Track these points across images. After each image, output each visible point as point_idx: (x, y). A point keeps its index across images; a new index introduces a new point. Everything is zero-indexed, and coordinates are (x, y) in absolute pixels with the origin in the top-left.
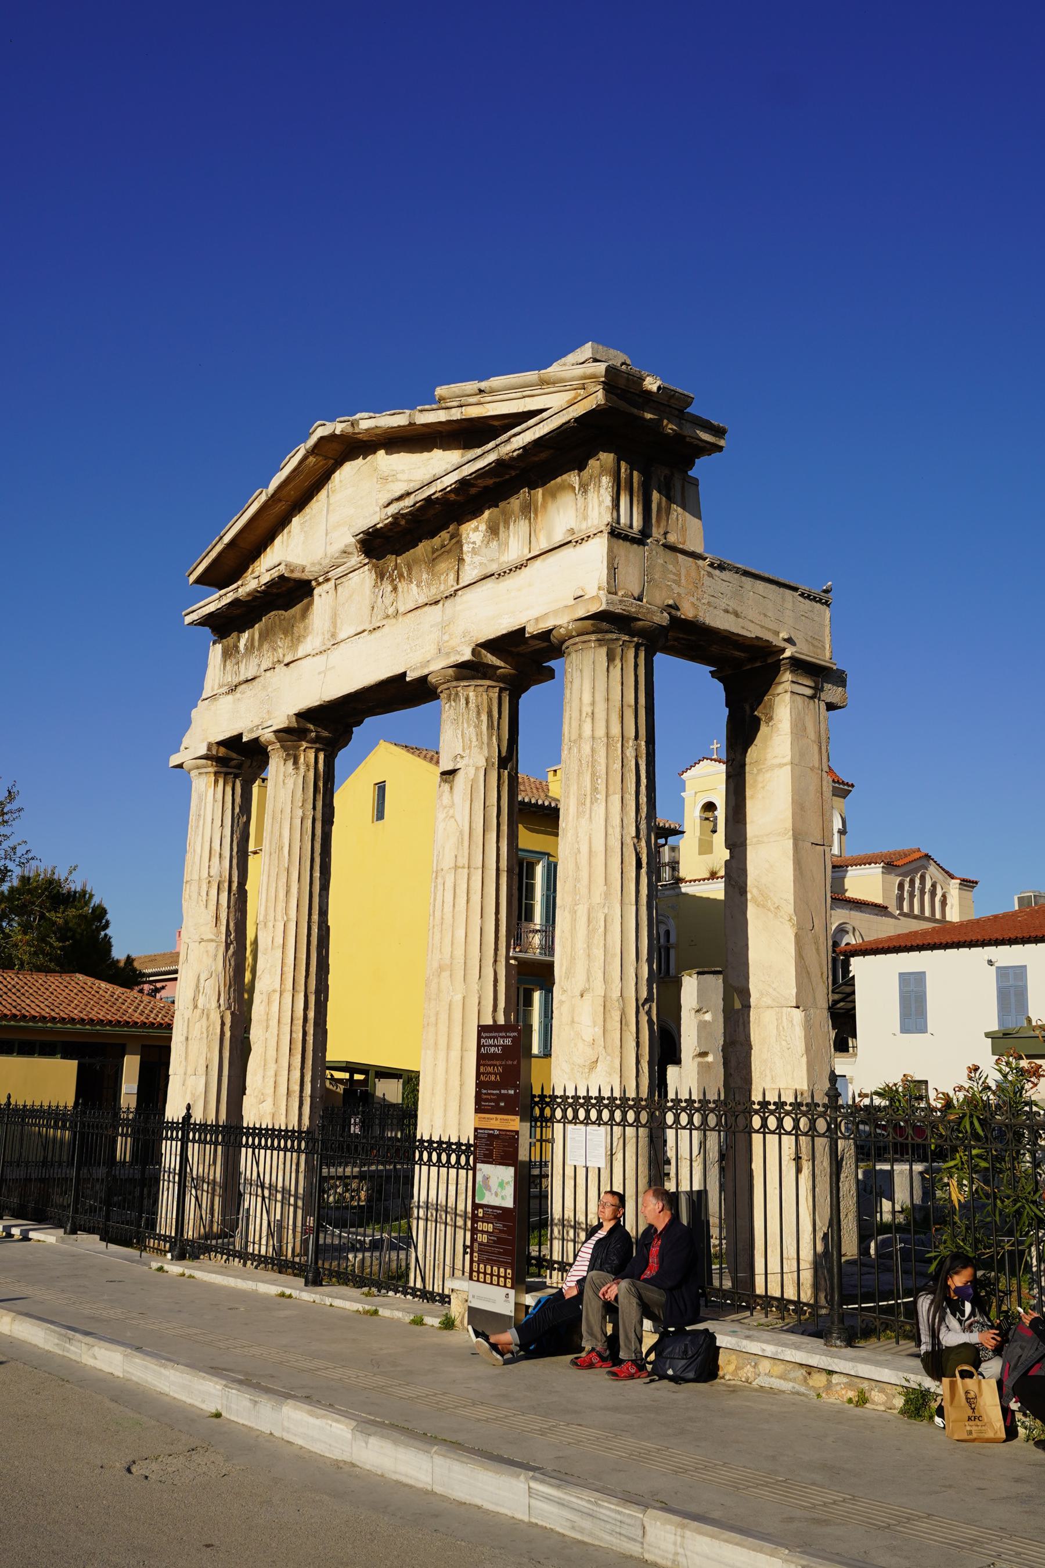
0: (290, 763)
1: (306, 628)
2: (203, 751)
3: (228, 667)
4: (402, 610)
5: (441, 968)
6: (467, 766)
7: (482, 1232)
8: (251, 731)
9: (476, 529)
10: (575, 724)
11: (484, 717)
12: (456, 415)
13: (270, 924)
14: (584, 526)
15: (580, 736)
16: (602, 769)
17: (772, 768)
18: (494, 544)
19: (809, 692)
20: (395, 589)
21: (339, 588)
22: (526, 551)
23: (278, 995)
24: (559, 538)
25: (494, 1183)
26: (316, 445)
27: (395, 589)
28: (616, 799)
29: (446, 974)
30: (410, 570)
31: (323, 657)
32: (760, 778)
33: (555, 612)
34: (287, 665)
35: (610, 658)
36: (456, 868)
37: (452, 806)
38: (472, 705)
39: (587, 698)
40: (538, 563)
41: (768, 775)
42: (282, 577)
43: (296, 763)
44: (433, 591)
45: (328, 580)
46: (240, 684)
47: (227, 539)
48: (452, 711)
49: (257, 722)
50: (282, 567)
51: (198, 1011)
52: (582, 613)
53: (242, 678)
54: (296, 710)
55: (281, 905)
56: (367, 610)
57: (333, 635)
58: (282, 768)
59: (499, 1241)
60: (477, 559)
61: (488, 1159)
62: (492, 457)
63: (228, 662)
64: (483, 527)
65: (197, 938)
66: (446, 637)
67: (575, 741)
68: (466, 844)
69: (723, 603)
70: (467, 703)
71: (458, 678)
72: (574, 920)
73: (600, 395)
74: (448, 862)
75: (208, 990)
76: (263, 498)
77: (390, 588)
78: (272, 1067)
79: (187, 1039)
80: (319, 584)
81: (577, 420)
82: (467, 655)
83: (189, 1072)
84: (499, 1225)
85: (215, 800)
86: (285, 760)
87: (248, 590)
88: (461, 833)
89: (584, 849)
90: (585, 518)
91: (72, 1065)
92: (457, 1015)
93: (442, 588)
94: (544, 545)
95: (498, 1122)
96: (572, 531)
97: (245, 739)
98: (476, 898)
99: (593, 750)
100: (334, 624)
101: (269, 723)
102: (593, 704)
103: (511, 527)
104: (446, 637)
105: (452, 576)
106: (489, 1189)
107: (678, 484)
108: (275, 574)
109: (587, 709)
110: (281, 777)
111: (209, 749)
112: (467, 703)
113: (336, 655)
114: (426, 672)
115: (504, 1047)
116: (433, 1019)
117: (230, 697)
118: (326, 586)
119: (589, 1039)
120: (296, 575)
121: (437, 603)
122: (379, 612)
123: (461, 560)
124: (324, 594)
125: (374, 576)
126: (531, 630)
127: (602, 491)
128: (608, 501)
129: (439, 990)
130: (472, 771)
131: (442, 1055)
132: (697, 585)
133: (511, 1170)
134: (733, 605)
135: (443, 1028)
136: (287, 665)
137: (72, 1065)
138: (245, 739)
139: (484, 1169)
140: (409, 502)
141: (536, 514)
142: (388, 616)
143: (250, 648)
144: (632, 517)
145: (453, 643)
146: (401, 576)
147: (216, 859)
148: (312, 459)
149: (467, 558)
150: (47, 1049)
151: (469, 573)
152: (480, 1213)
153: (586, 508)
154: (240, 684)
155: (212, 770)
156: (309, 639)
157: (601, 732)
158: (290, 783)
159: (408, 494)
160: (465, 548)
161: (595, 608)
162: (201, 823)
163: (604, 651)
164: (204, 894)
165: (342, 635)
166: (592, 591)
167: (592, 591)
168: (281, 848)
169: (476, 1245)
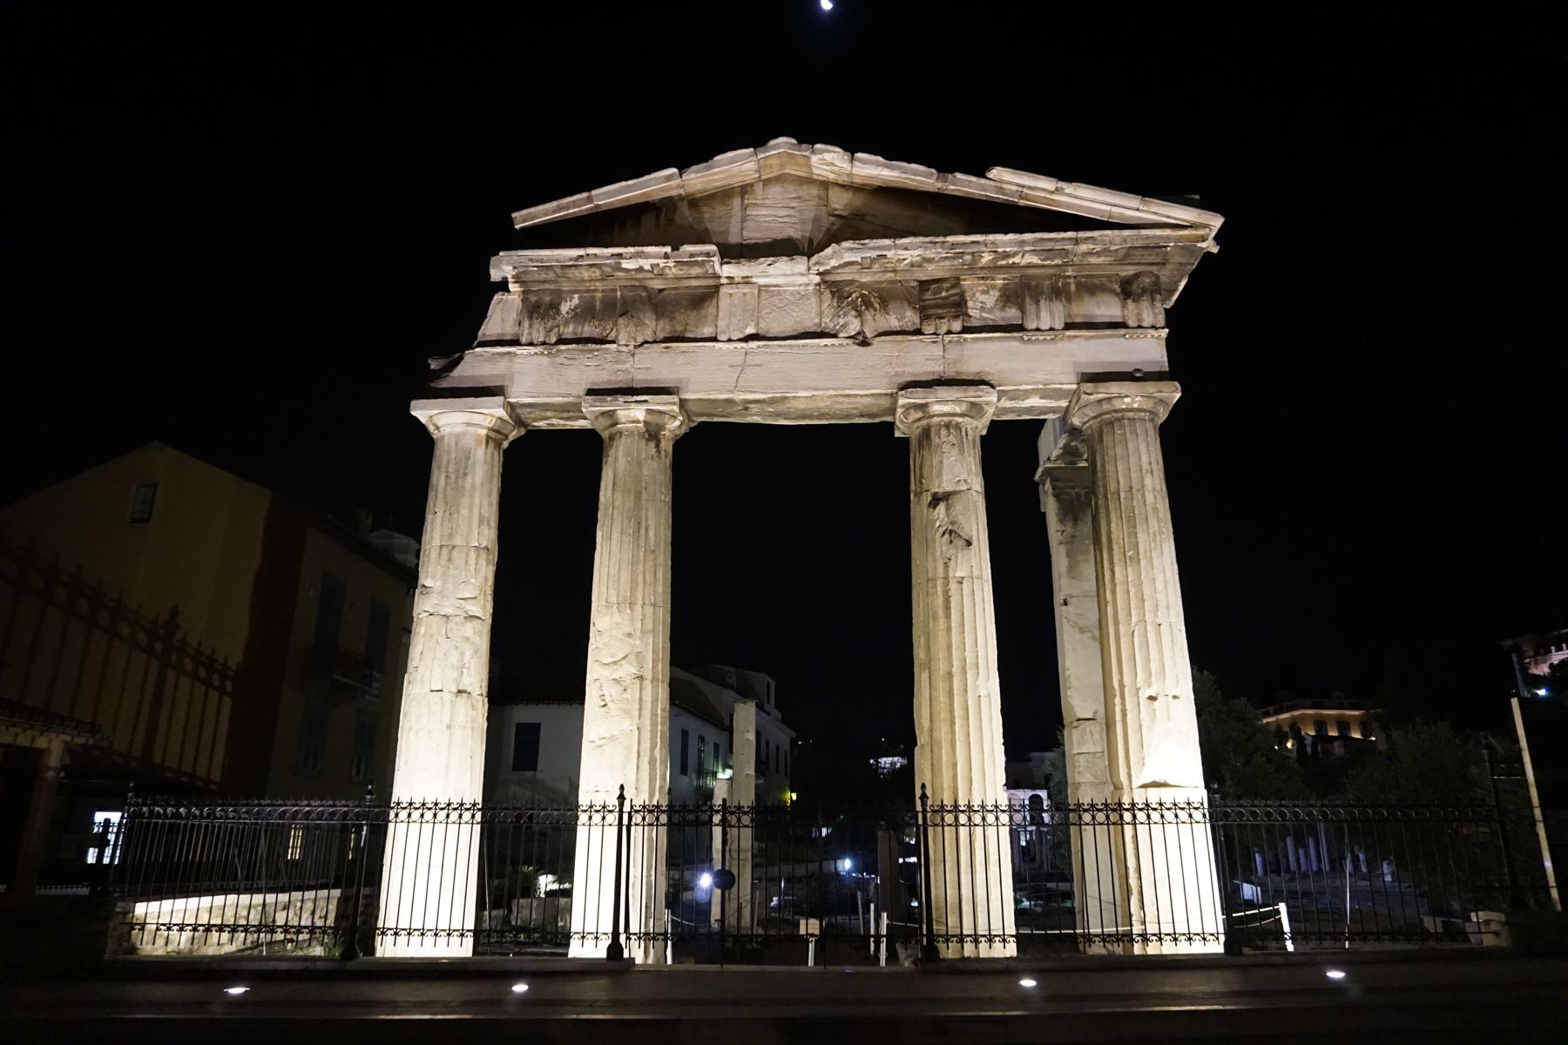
9: (986, 292)
13: (638, 608)
20: (860, 315)
43: (657, 446)
64: (995, 294)
71: (962, 415)
79: (449, 727)
90: (1139, 316)
117: (545, 360)
160: (970, 304)
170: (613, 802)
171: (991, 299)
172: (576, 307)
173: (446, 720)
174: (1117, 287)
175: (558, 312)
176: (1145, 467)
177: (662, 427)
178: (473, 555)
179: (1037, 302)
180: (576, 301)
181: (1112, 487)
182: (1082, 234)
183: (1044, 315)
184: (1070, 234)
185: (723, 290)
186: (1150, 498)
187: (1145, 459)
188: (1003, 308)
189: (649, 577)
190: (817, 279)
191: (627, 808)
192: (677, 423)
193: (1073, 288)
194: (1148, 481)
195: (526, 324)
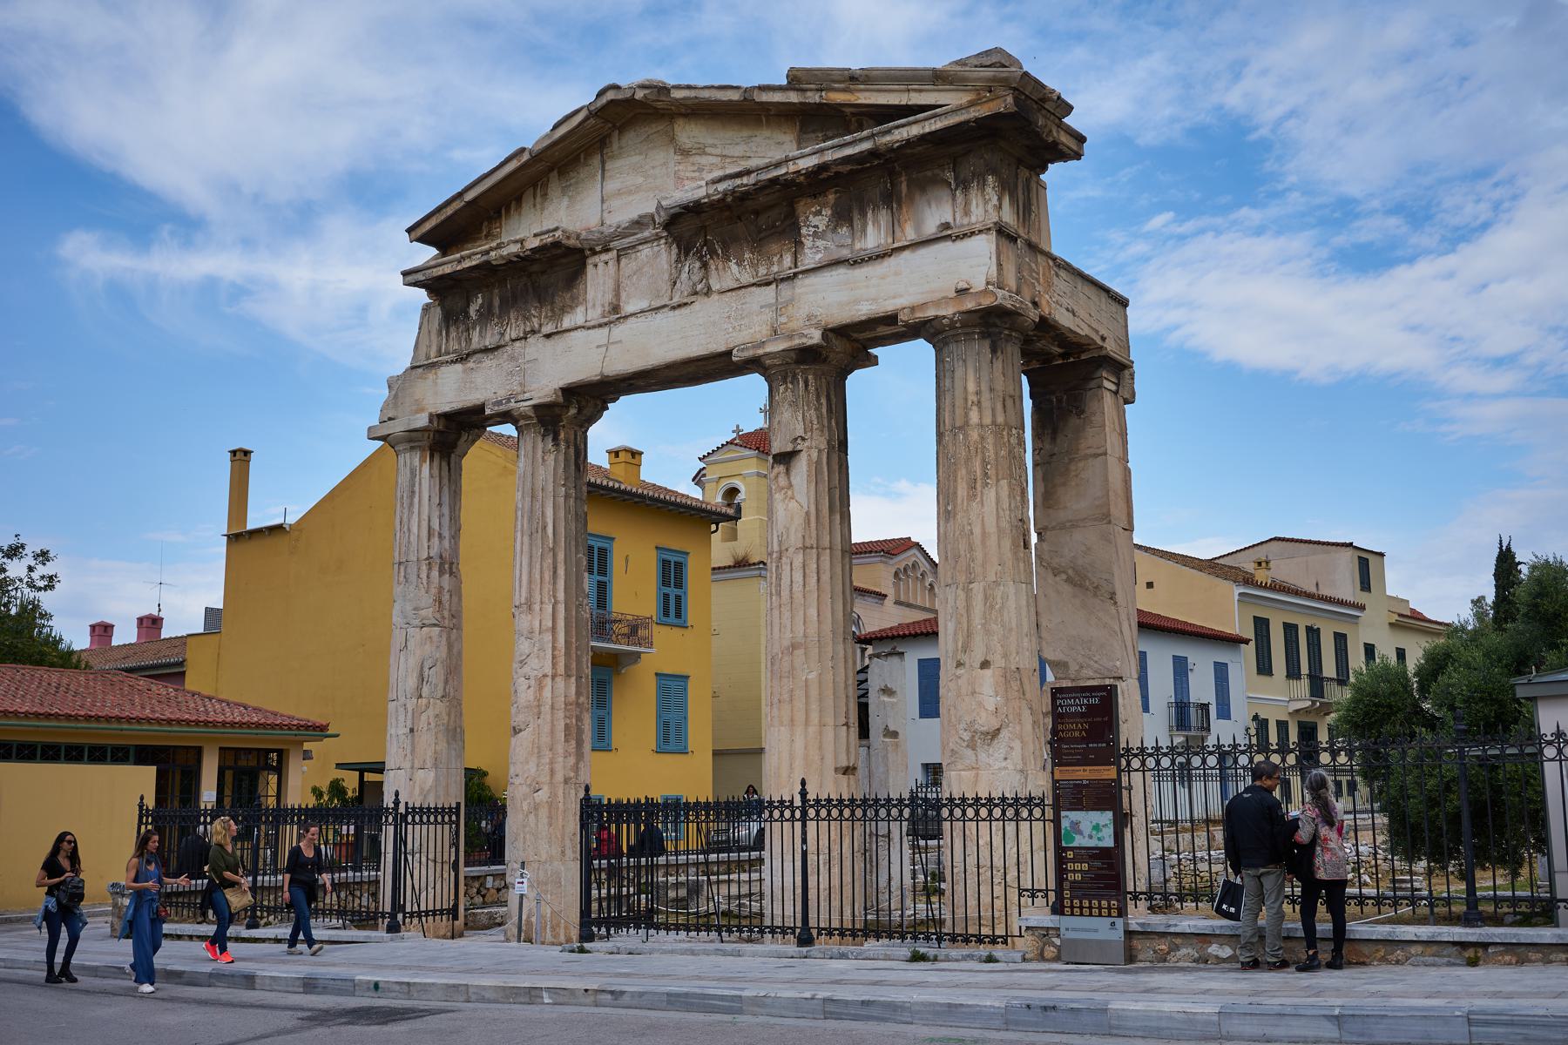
0: (549, 439)
1: (573, 299)
2: (422, 421)
3: (453, 334)
4: (715, 286)
5: (794, 646)
6: (810, 448)
7: (1074, 871)
8: (499, 403)
9: (818, 213)
10: (959, 412)
11: (823, 401)
12: (813, 98)
13: (537, 607)
14: (965, 221)
15: (967, 423)
16: (991, 454)
17: (1086, 457)
18: (844, 230)
19: (1113, 388)
20: (705, 266)
21: (624, 261)
22: (890, 240)
23: (549, 680)
24: (931, 227)
25: (1086, 827)
26: (603, 108)
27: (705, 266)
28: (1004, 483)
29: (799, 652)
30: (725, 248)
31: (605, 330)
32: (1073, 467)
33: (937, 303)
34: (548, 336)
35: (994, 351)
36: (805, 548)
37: (790, 486)
38: (812, 389)
39: (971, 387)
40: (906, 253)
41: (1081, 465)
42: (556, 244)
43: (555, 439)
44: (762, 271)
45: (607, 250)
46: (475, 352)
48: (789, 393)
49: (502, 394)
50: (557, 234)
51: (423, 701)
52: (970, 305)
53: (475, 344)
54: (562, 383)
55: (548, 587)
56: (665, 287)
57: (616, 308)
58: (540, 445)
59: (1098, 877)
60: (820, 243)
61: (1077, 805)
62: (866, 146)
63: (452, 329)
64: (827, 212)
65: (417, 622)
66: (783, 319)
67: (960, 428)
68: (813, 525)
69: (1065, 301)
70: (806, 386)
71: (799, 362)
72: (968, 599)
73: (1010, 99)
74: (795, 540)
75: (433, 680)
77: (698, 264)
78: (547, 755)
79: (412, 730)
80: (594, 253)
81: (977, 120)
82: (815, 337)
83: (417, 765)
84: (1098, 864)
85: (431, 476)
86: (544, 436)
88: (807, 513)
89: (977, 531)
90: (967, 213)
91: (151, 771)
92: (814, 693)
93: (775, 269)
94: (910, 234)
95: (1084, 774)
96: (946, 226)
98: (826, 577)
99: (982, 438)
100: (617, 295)
101: (527, 396)
102: (978, 393)
103: (870, 215)
104: (783, 319)
105: (788, 260)
106: (1080, 833)
107: (1034, 185)
109: (972, 398)
110: (540, 453)
111: (431, 421)
112: (806, 386)
113: (620, 331)
114: (760, 352)
115: (1088, 706)
116: (786, 696)
117: (459, 367)
118: (604, 257)
119: (991, 708)
120: (572, 242)
121: (768, 284)
122: (684, 285)
123: (799, 244)
124: (601, 265)
125: (675, 250)
127: (989, 190)
128: (995, 200)
129: (793, 668)
130: (815, 455)
131: (799, 730)
132: (1049, 285)
133: (1110, 814)
134: (1072, 305)
135: (799, 704)
136: (548, 336)
137: (151, 771)
138: (488, 412)
139: (1069, 817)
140: (752, 179)
141: (900, 205)
142: (696, 293)
143: (486, 315)
144: (1008, 216)
145: (793, 325)
146: (713, 253)
147: (436, 540)
148: (592, 121)
149: (808, 242)
150: (119, 755)
151: (810, 258)
152: (1070, 855)
153: (967, 204)
154: (475, 352)
155: (426, 443)
156: (580, 310)
157: (987, 420)
158: (551, 459)
159: (748, 172)
160: (804, 231)
161: (987, 302)
162: (416, 500)
163: (987, 343)
164: (424, 576)
165: (628, 308)
166: (979, 284)
167: (979, 284)
168: (545, 528)
169: (1066, 885)
170: (391, 805)
171: (821, 222)
172: (482, 306)
173: (409, 725)
174: (950, 176)
175: (467, 316)
176: (972, 398)
177: (558, 418)
178: (424, 568)
179: (863, 215)
180: (480, 301)
183: (870, 228)
184: (865, 133)
185: (590, 261)
186: (974, 435)
187: (971, 387)
188: (834, 230)
189: (548, 576)
191: (402, 810)
192: (573, 411)
193: (904, 187)
194: (974, 417)
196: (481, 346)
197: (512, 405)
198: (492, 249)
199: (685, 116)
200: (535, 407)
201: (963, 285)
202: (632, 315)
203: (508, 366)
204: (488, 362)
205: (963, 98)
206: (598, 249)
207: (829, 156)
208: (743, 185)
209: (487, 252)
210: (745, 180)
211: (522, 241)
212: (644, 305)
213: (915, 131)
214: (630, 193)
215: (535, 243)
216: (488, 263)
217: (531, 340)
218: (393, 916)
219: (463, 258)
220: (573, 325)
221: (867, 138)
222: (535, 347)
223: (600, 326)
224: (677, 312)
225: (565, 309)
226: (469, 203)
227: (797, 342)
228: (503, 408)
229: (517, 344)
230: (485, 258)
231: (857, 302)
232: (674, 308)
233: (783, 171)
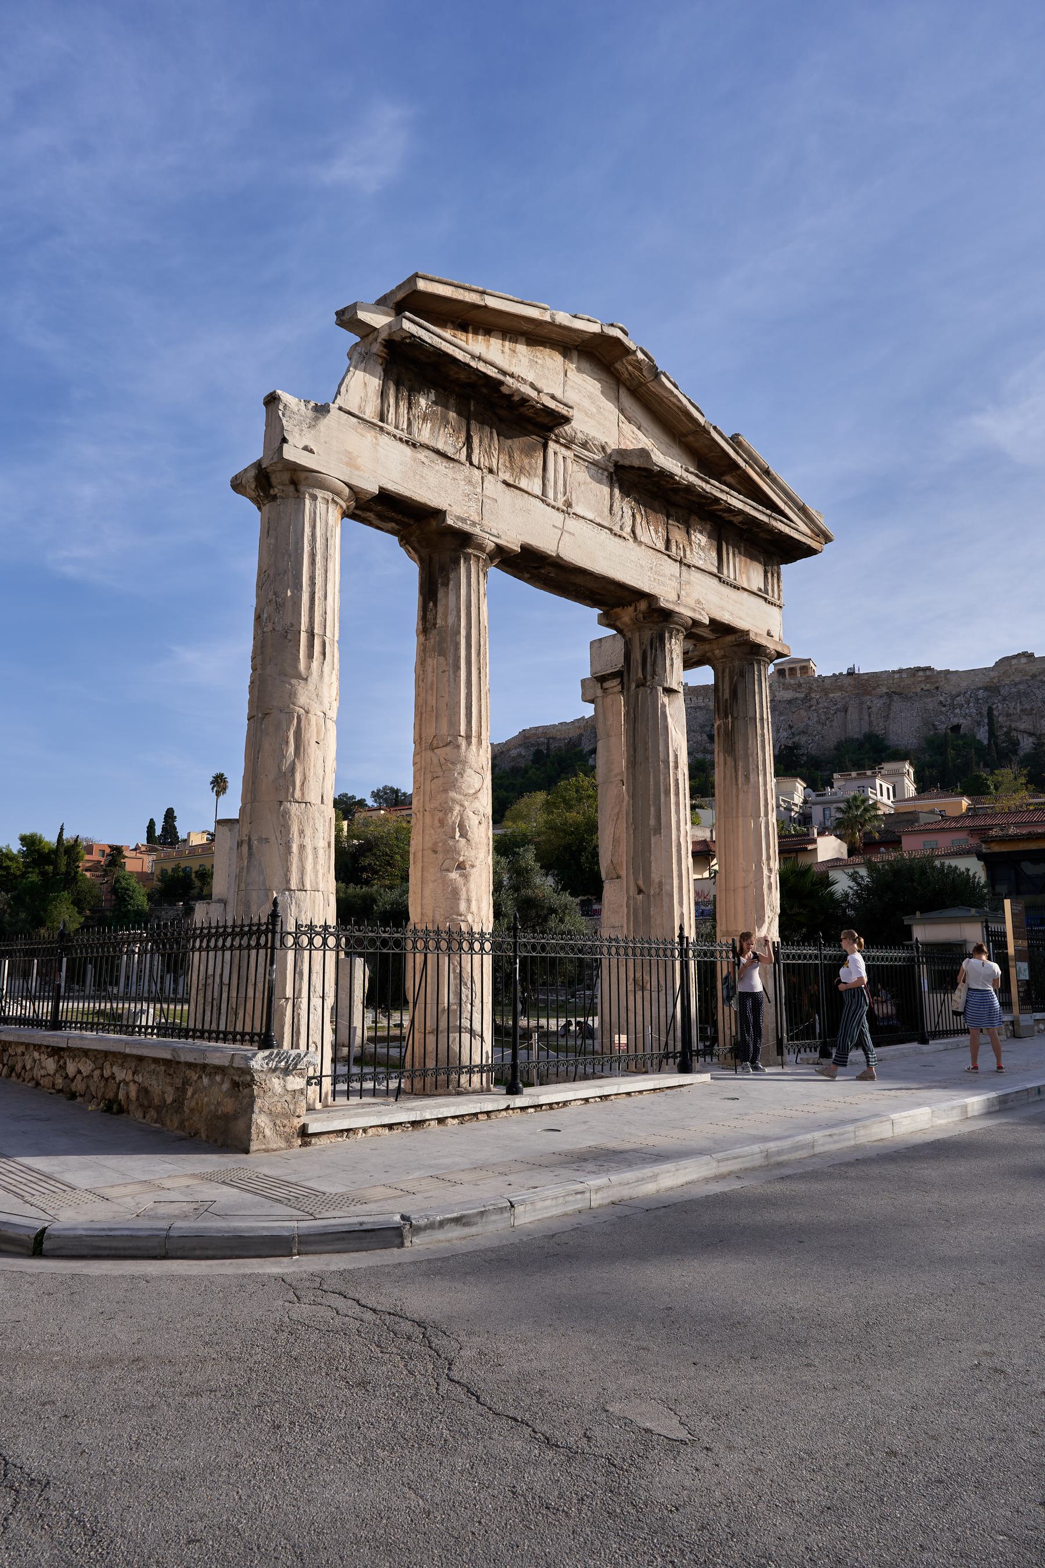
9: (701, 532)
31: (561, 516)
40: (746, 593)
46: (428, 447)
47: (492, 302)
76: (547, 317)
80: (557, 442)
87: (522, 389)
96: (760, 590)
97: (450, 521)
108: (564, 411)
114: (677, 609)
117: (407, 450)
118: (563, 449)
121: (676, 561)
126: (752, 636)
154: (428, 447)
181: (750, 714)
182: (774, 514)
184: (768, 512)
190: (612, 470)
195: (392, 401)
196: (432, 443)
197: (476, 530)
198: (512, 376)
199: (629, 389)
200: (497, 545)
201: (772, 633)
202: (583, 518)
203: (468, 489)
204: (441, 465)
205: (809, 532)
206: (562, 441)
207: (748, 509)
208: (702, 488)
209: (504, 373)
210: (704, 485)
211: (539, 392)
212: (590, 516)
213: (786, 530)
214: (586, 414)
215: (552, 404)
216: (501, 383)
217: (490, 477)
218: (683, 1054)
219: (480, 358)
220: (529, 490)
221: (767, 515)
222: (493, 486)
223: (558, 509)
224: (617, 539)
225: (522, 470)
226: (486, 307)
227: (697, 616)
228: (467, 528)
229: (476, 472)
230: (500, 377)
231: (722, 608)
232: (615, 534)
233: (723, 496)
